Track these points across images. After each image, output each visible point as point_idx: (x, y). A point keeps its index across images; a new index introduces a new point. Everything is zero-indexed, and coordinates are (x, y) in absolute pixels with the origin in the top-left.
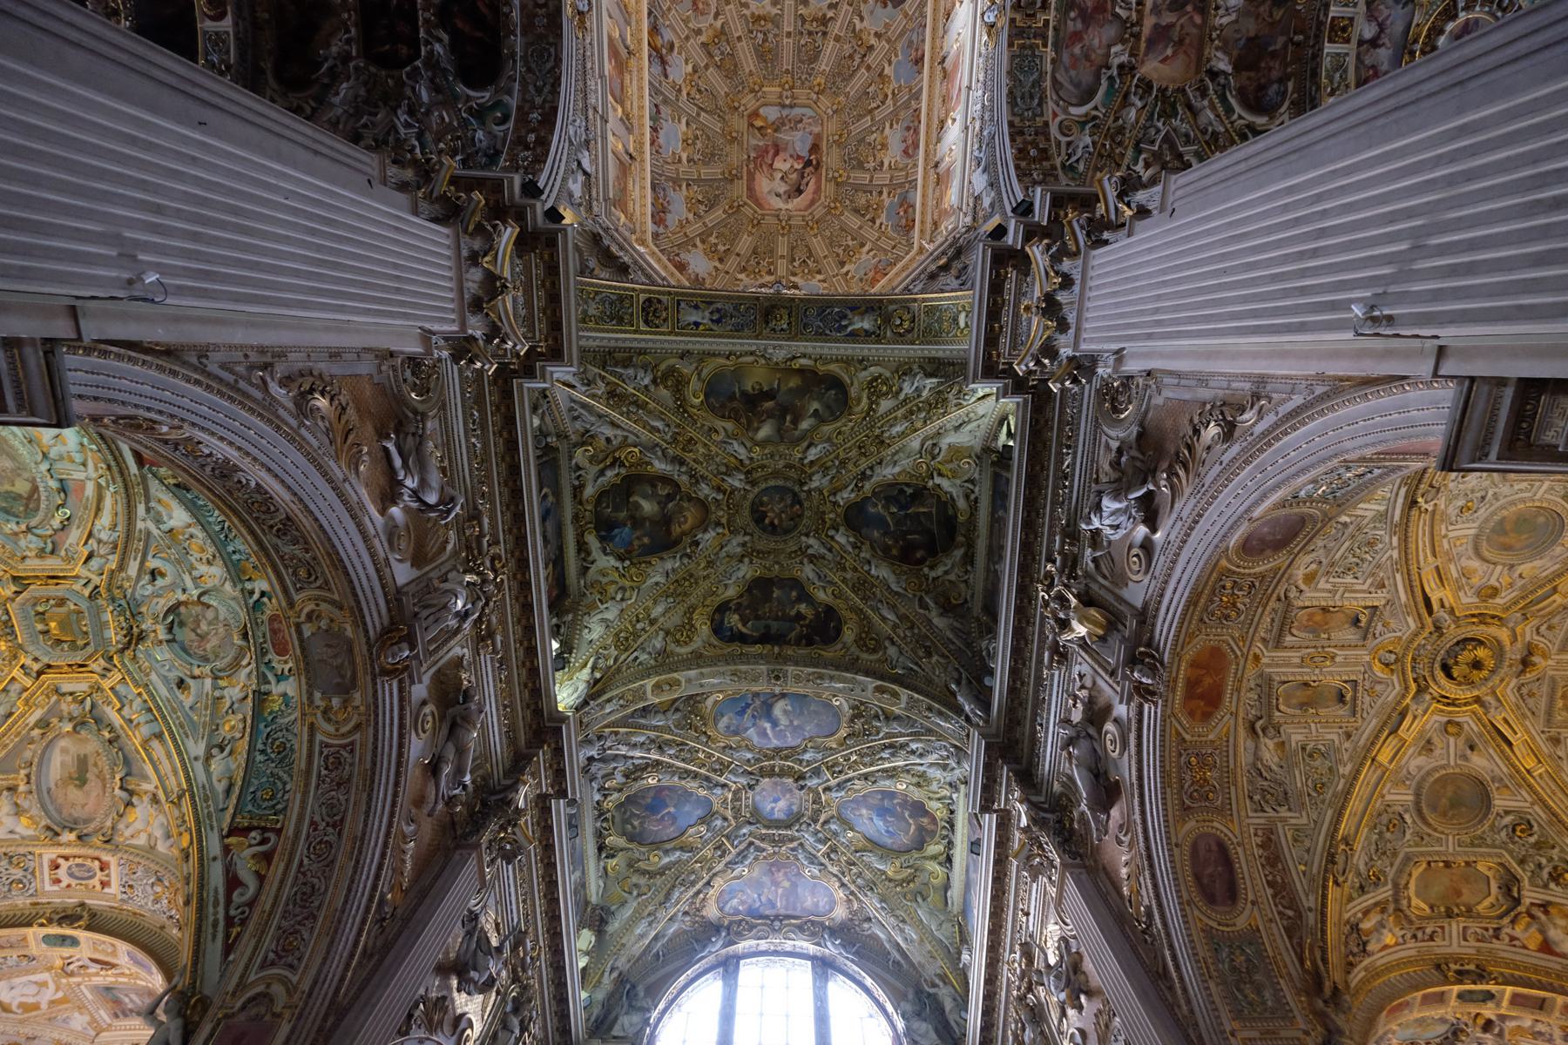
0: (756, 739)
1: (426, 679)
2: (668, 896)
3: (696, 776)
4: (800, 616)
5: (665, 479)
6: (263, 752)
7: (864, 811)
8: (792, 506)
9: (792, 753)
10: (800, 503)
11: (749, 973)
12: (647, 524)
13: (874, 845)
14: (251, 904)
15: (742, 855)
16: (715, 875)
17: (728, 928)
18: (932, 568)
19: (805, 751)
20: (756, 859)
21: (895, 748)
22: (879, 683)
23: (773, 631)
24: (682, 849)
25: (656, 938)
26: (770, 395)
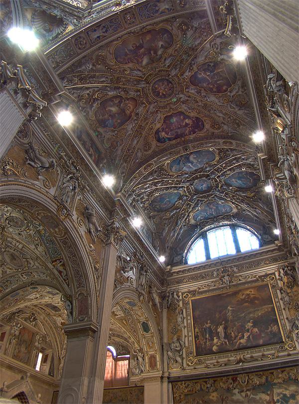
0: (187, 170)
1: (74, 213)
2: (177, 223)
3: (171, 188)
4: (187, 125)
5: (116, 97)
6: (47, 243)
7: (233, 180)
8: (168, 85)
9: (201, 170)
10: (171, 83)
11: (211, 235)
12: (117, 115)
13: (240, 189)
14: (67, 275)
15: (196, 205)
16: (190, 212)
17: (200, 225)
18: (230, 92)
19: (206, 168)
20: (202, 204)
21: (237, 159)
22: (224, 140)
23: (179, 133)
24: (176, 209)
25: (178, 235)
26: (141, 46)
